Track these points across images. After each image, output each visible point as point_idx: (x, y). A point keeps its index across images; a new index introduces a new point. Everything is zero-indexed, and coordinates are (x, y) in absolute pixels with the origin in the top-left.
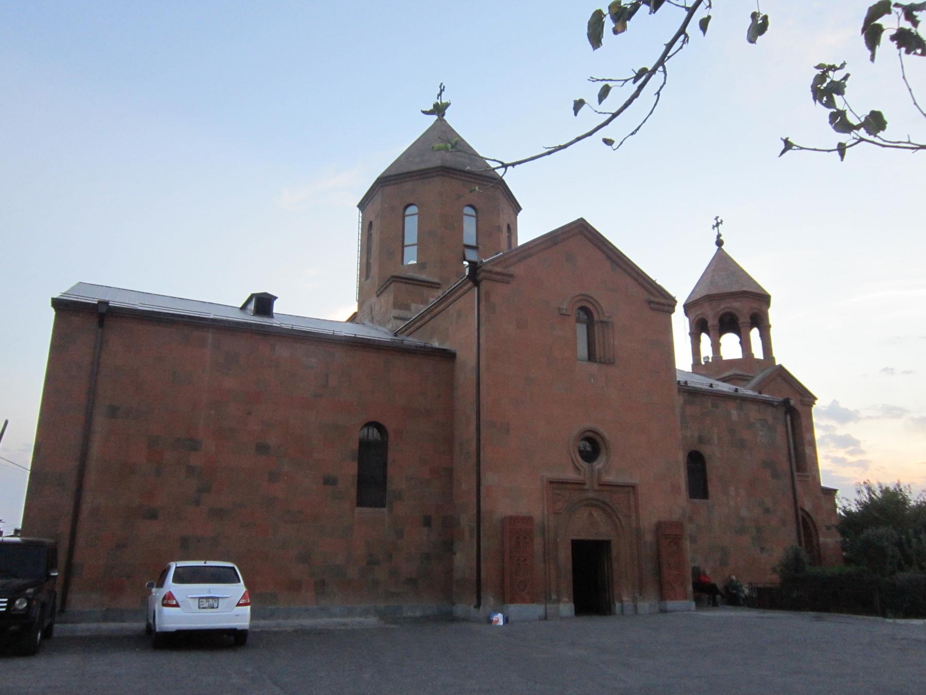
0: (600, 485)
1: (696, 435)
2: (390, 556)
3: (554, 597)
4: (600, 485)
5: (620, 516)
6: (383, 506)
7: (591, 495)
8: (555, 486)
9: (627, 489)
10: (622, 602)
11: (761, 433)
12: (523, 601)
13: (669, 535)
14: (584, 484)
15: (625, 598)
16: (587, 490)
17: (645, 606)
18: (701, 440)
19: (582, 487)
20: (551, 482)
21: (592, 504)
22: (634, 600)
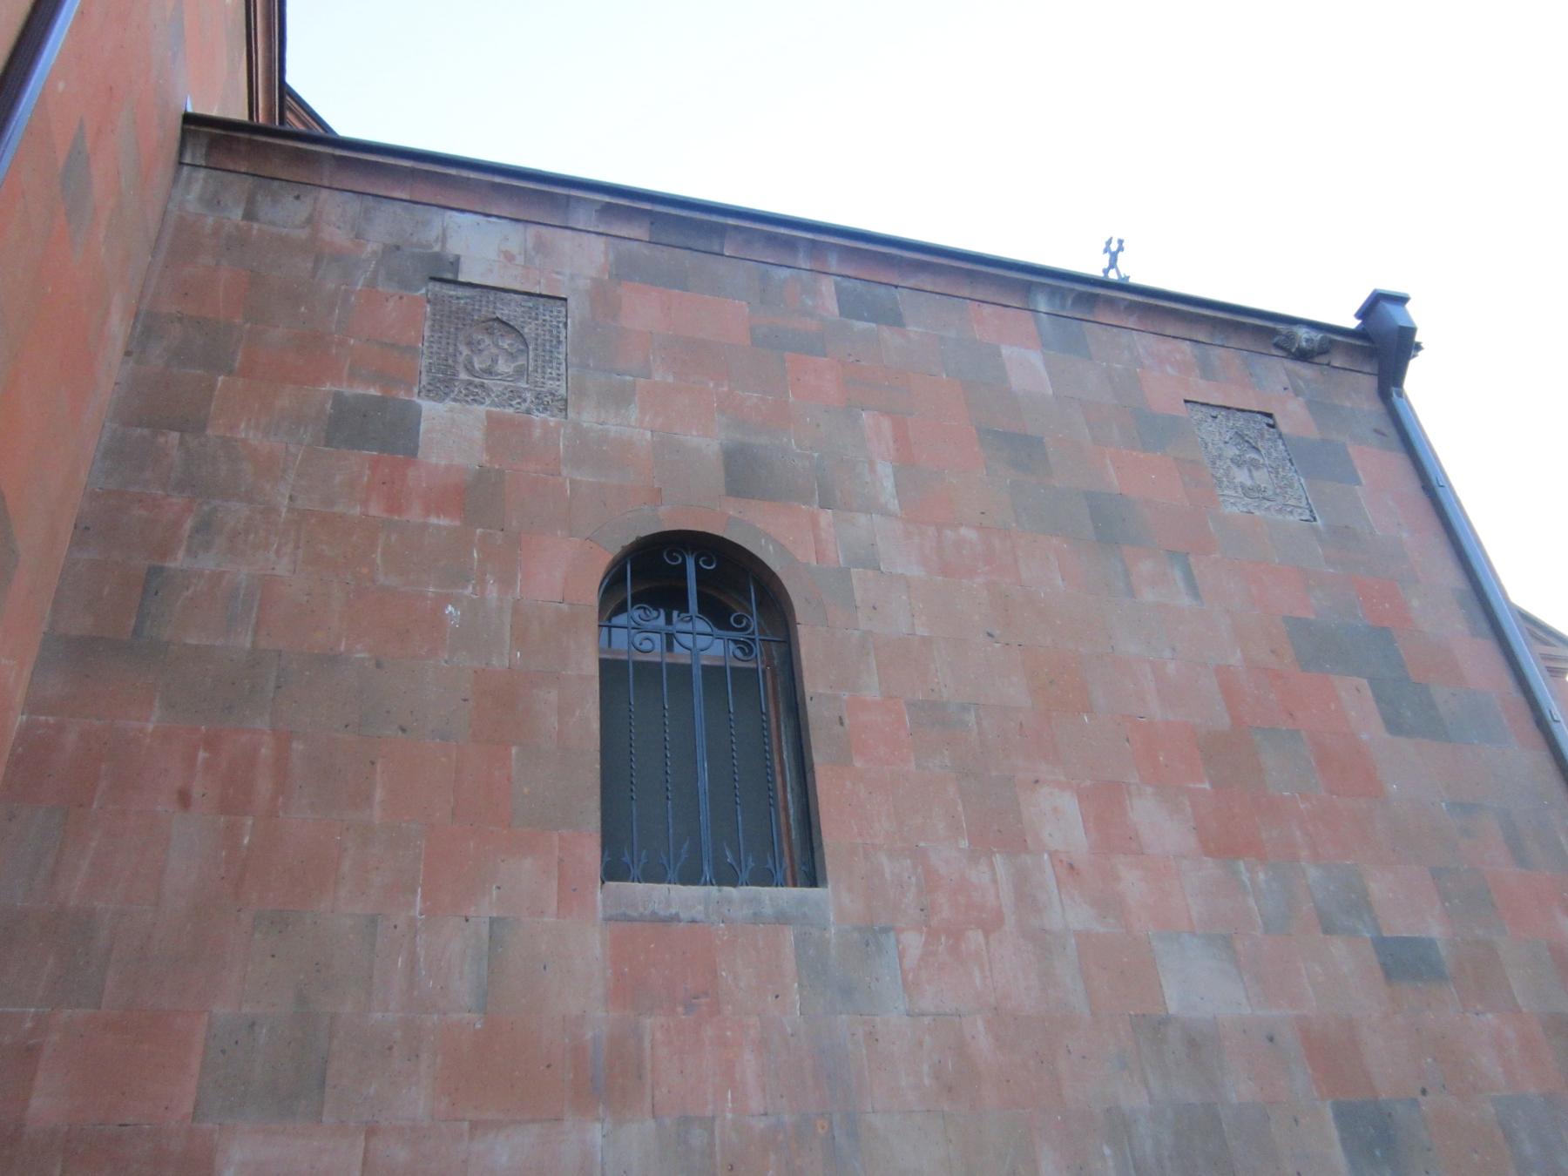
1: (706, 442)
11: (1241, 476)
18: (744, 472)
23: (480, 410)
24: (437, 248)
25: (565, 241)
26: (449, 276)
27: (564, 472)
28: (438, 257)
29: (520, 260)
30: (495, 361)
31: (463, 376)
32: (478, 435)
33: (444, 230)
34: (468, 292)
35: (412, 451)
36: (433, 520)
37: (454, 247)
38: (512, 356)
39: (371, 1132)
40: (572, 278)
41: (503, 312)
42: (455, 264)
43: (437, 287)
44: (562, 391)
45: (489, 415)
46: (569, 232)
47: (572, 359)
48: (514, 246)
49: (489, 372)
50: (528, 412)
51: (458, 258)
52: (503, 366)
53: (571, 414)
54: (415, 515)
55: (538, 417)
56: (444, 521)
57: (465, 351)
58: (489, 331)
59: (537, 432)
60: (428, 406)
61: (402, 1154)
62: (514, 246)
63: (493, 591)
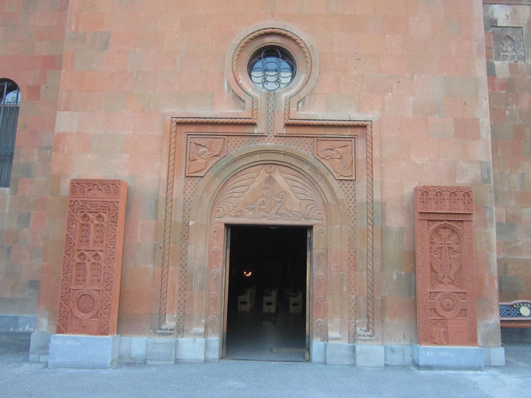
0: (287, 125)
2: (9, 250)
3: (170, 323)
4: (287, 125)
5: (330, 178)
6: (7, 185)
7: (269, 144)
8: (192, 129)
9: (348, 132)
10: (325, 338)
12: (84, 329)
13: (444, 215)
14: (254, 124)
15: (332, 334)
16: (262, 136)
17: (373, 352)
19: (248, 130)
20: (179, 124)
21: (271, 161)
22: (353, 337)
23: (507, 62)
24: (491, 17)
25: (520, 8)
26: (495, 25)
27: (526, 76)
28: (492, 19)
29: (510, 17)
30: (507, 48)
31: (502, 53)
32: (508, 69)
33: (492, 11)
34: (499, 29)
35: (495, 75)
36: (501, 92)
37: (495, 16)
38: (511, 46)
39: (506, 207)
40: (523, 20)
41: (509, 33)
42: (496, 21)
43: (493, 29)
44: (523, 55)
45: (510, 65)
46: (520, 6)
47: (525, 46)
48: (508, 13)
49: (507, 51)
50: (516, 62)
51: (496, 19)
52: (510, 49)
53: (526, 61)
54: (497, 91)
55: (519, 62)
56: (503, 92)
57: (501, 46)
58: (505, 39)
59: (519, 67)
60: (496, 63)
61: (511, 211)
62: (508, 13)
63: (515, 107)
